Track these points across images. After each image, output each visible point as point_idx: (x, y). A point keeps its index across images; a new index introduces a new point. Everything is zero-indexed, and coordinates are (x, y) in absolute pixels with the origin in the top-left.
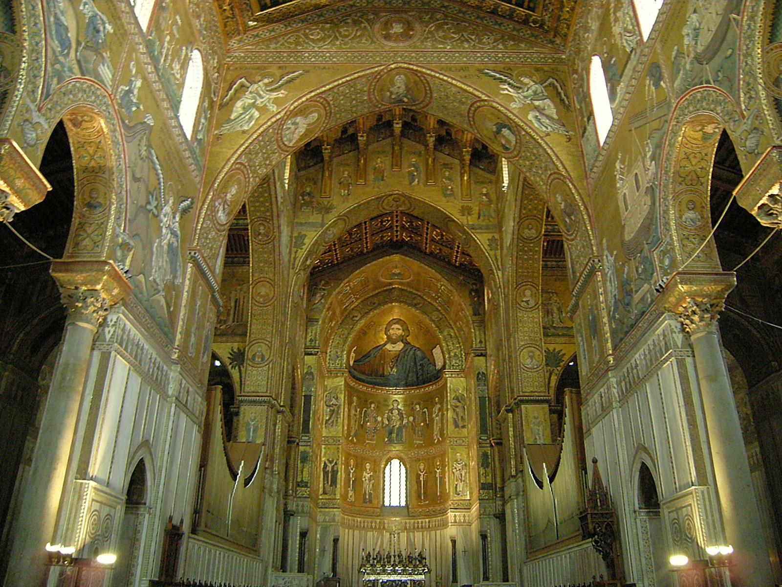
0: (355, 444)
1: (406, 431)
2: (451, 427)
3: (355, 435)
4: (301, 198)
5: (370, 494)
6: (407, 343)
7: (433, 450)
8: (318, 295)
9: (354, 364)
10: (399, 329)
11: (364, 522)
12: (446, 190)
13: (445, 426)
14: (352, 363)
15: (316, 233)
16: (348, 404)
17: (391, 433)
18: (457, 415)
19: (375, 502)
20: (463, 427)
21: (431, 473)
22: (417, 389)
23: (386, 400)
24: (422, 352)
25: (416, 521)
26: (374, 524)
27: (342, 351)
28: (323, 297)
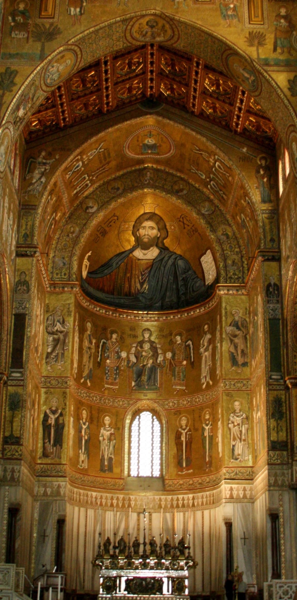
0: (89, 388)
1: (161, 372)
2: (227, 364)
3: (90, 376)
4: (10, 18)
5: (110, 459)
6: (163, 249)
7: (200, 399)
8: (37, 172)
9: (87, 276)
10: (153, 228)
11: (101, 498)
12: (227, 10)
13: (218, 364)
14: (85, 274)
15: (32, 68)
16: (80, 333)
17: (139, 374)
18: (236, 347)
19: (116, 470)
20: (245, 364)
21: (196, 430)
22: (178, 312)
23: (133, 329)
24: (187, 262)
25: (175, 497)
26: (115, 502)
27: (71, 257)
28: (43, 174)
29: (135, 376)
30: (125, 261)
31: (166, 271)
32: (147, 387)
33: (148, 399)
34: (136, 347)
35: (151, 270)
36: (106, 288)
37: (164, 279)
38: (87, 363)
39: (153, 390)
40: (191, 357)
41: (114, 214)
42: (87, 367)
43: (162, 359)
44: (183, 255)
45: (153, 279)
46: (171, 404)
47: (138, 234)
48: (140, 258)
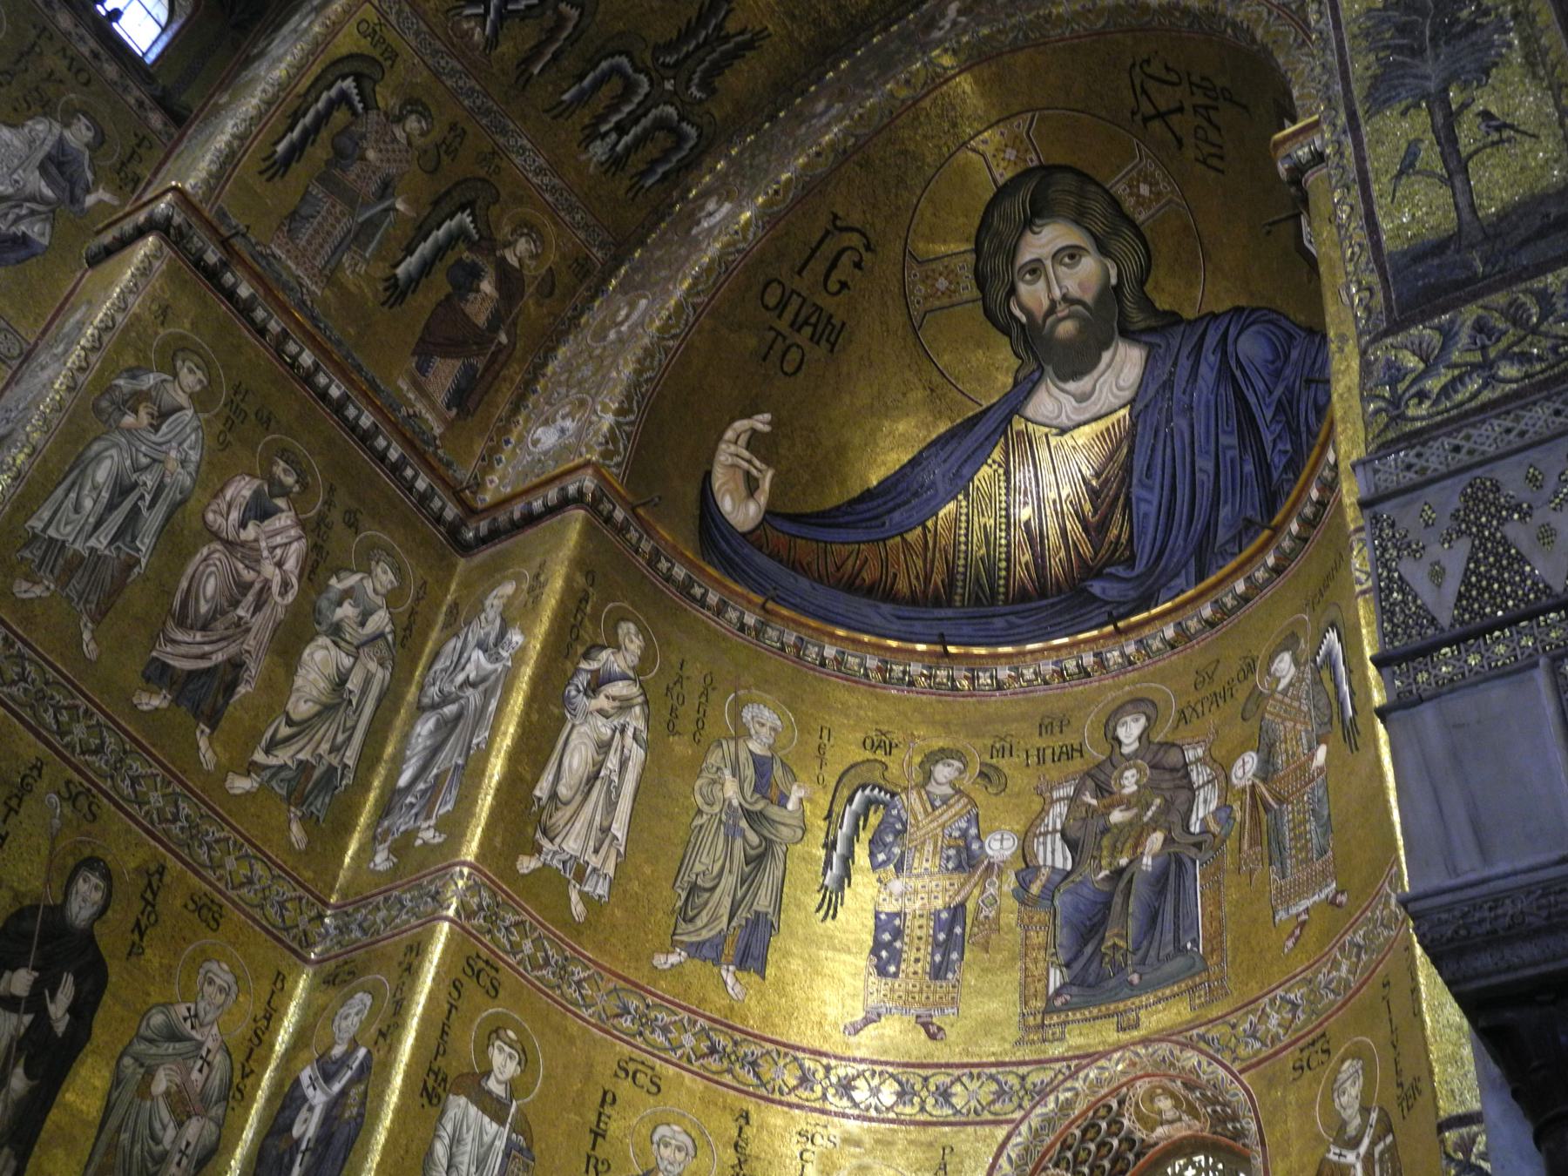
10: (1072, 254)
29: (1063, 936)
30: (997, 454)
31: (1200, 429)
32: (1135, 978)
33: (1145, 1041)
34: (1073, 800)
35: (1131, 451)
36: (902, 585)
37: (1199, 463)
38: (729, 881)
39: (1173, 979)
40: (1342, 705)
41: (836, 217)
42: (722, 899)
43: (1213, 806)
44: (1243, 302)
45: (1151, 489)
46: (1274, 1020)
47: (1017, 312)
48: (1064, 421)
